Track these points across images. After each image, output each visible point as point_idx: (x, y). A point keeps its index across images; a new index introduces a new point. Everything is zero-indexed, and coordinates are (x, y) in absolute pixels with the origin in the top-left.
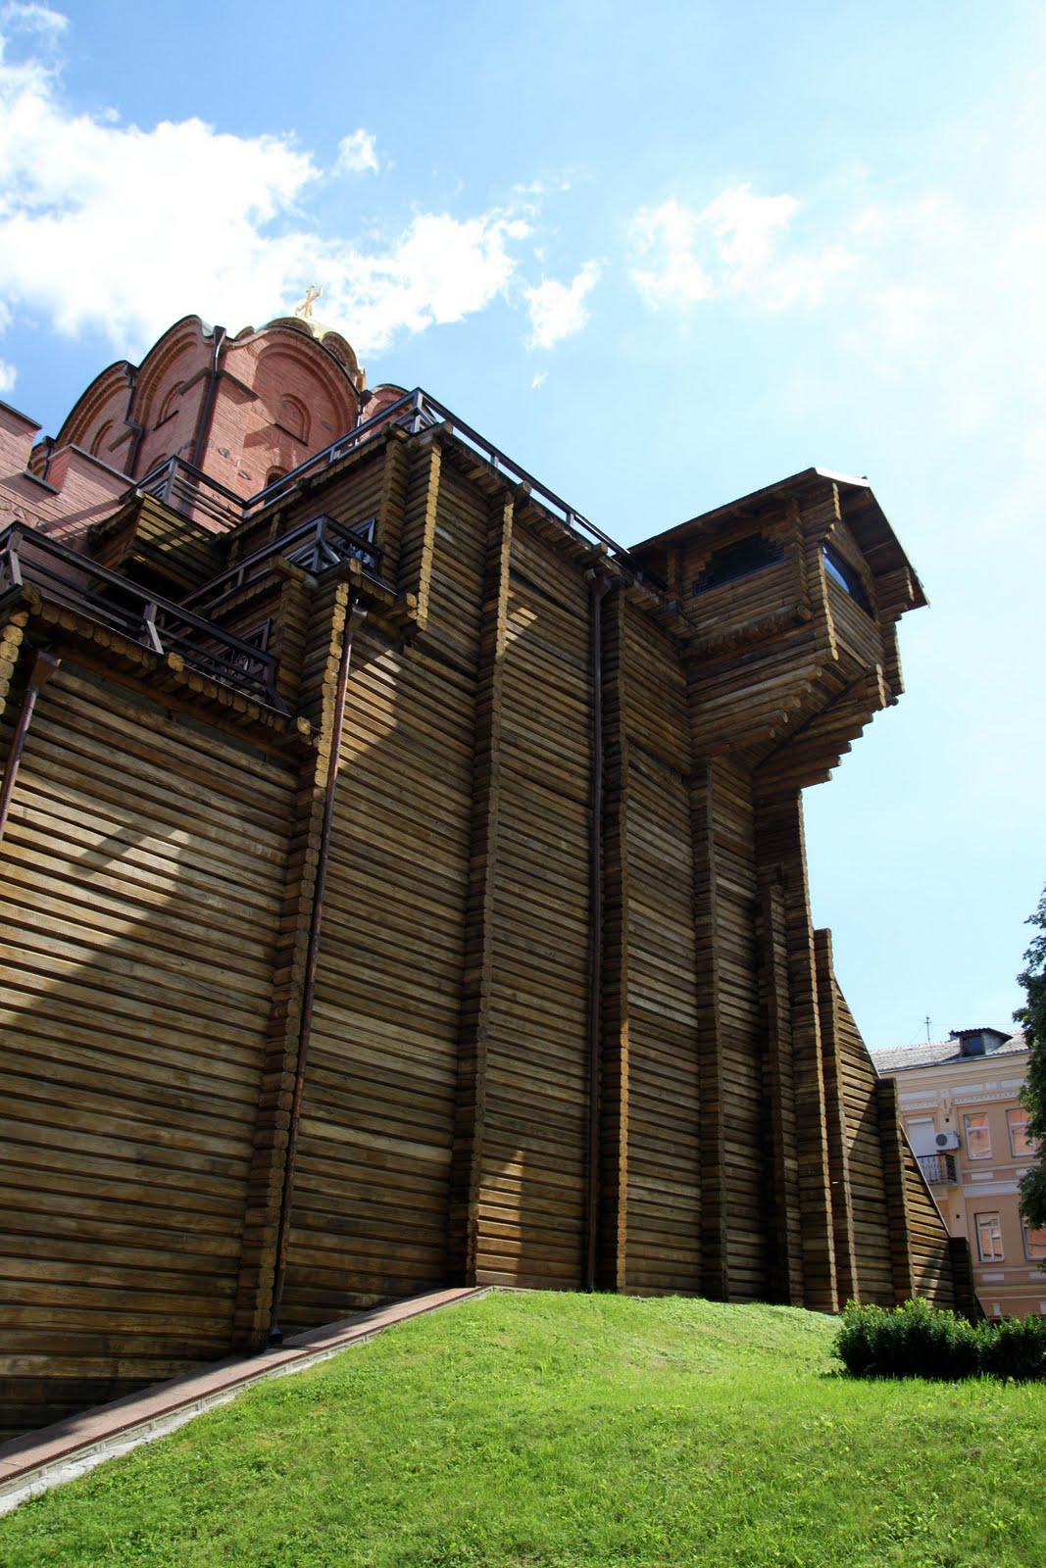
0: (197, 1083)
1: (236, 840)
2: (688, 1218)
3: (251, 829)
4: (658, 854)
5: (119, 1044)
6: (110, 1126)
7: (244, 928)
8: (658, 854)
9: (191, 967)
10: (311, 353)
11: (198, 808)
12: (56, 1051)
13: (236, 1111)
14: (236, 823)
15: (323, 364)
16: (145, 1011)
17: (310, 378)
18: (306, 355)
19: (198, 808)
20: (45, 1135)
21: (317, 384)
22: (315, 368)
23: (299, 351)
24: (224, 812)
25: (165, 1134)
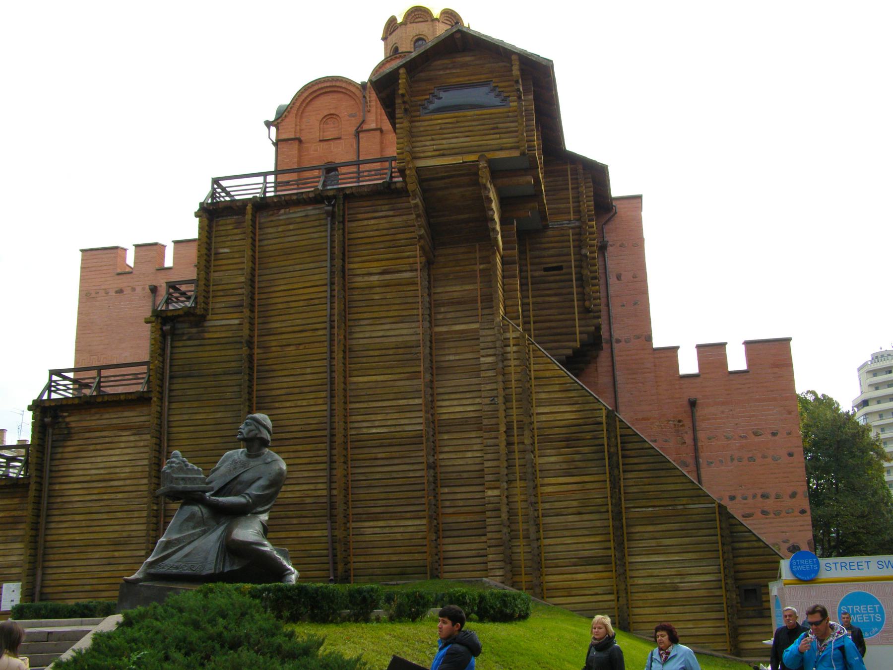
0: (125, 534)
1: (132, 444)
3: (137, 438)
4: (393, 339)
5: (97, 529)
6: (97, 555)
7: (139, 475)
8: (393, 339)
9: (120, 496)
10: (328, 84)
11: (116, 439)
12: (77, 537)
13: (142, 540)
14: (132, 438)
15: (338, 84)
16: (105, 516)
17: (336, 96)
18: (327, 87)
19: (116, 439)
20: (77, 563)
21: (341, 95)
22: (336, 89)
23: (322, 88)
24: (126, 437)
25: (116, 554)
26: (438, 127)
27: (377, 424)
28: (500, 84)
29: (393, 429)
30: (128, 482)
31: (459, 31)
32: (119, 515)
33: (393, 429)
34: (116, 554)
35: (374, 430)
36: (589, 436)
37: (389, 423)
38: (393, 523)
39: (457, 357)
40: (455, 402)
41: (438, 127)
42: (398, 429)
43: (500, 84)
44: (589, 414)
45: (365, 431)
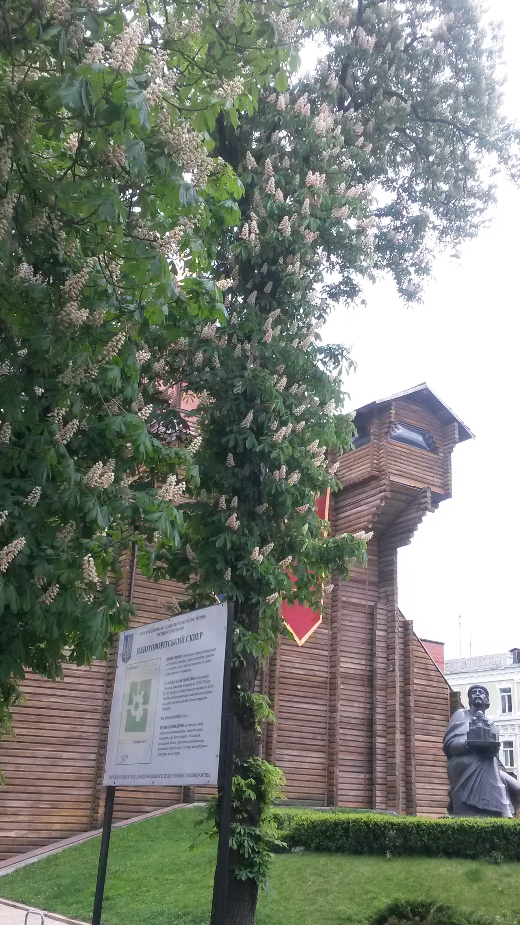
2: (321, 767)
25: (65, 755)
26: (399, 453)
27: (297, 665)
28: (435, 437)
29: (307, 672)
30: (83, 681)
31: (427, 389)
32: (71, 714)
33: (307, 672)
34: (65, 755)
35: (294, 671)
36: (440, 707)
37: (305, 666)
38: (304, 753)
39: (352, 624)
40: (349, 660)
41: (399, 453)
42: (311, 673)
43: (435, 437)
44: (440, 690)
45: (288, 670)
